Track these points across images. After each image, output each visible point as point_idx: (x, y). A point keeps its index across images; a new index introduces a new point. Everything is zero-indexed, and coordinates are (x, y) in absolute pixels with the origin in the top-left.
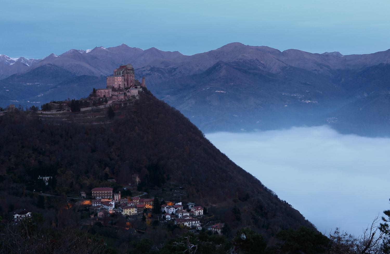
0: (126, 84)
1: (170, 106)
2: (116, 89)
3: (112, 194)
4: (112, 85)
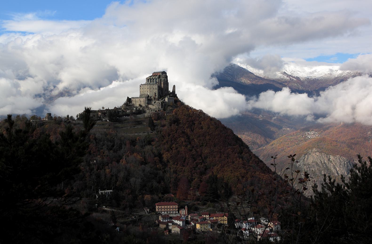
0: (161, 92)
1: (210, 116)
2: (151, 98)
3: (177, 209)
4: (146, 94)
